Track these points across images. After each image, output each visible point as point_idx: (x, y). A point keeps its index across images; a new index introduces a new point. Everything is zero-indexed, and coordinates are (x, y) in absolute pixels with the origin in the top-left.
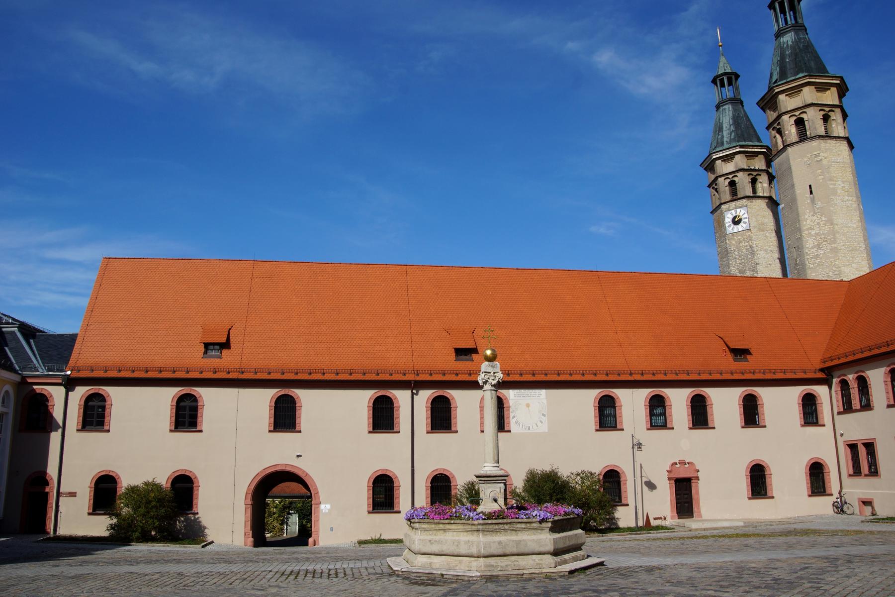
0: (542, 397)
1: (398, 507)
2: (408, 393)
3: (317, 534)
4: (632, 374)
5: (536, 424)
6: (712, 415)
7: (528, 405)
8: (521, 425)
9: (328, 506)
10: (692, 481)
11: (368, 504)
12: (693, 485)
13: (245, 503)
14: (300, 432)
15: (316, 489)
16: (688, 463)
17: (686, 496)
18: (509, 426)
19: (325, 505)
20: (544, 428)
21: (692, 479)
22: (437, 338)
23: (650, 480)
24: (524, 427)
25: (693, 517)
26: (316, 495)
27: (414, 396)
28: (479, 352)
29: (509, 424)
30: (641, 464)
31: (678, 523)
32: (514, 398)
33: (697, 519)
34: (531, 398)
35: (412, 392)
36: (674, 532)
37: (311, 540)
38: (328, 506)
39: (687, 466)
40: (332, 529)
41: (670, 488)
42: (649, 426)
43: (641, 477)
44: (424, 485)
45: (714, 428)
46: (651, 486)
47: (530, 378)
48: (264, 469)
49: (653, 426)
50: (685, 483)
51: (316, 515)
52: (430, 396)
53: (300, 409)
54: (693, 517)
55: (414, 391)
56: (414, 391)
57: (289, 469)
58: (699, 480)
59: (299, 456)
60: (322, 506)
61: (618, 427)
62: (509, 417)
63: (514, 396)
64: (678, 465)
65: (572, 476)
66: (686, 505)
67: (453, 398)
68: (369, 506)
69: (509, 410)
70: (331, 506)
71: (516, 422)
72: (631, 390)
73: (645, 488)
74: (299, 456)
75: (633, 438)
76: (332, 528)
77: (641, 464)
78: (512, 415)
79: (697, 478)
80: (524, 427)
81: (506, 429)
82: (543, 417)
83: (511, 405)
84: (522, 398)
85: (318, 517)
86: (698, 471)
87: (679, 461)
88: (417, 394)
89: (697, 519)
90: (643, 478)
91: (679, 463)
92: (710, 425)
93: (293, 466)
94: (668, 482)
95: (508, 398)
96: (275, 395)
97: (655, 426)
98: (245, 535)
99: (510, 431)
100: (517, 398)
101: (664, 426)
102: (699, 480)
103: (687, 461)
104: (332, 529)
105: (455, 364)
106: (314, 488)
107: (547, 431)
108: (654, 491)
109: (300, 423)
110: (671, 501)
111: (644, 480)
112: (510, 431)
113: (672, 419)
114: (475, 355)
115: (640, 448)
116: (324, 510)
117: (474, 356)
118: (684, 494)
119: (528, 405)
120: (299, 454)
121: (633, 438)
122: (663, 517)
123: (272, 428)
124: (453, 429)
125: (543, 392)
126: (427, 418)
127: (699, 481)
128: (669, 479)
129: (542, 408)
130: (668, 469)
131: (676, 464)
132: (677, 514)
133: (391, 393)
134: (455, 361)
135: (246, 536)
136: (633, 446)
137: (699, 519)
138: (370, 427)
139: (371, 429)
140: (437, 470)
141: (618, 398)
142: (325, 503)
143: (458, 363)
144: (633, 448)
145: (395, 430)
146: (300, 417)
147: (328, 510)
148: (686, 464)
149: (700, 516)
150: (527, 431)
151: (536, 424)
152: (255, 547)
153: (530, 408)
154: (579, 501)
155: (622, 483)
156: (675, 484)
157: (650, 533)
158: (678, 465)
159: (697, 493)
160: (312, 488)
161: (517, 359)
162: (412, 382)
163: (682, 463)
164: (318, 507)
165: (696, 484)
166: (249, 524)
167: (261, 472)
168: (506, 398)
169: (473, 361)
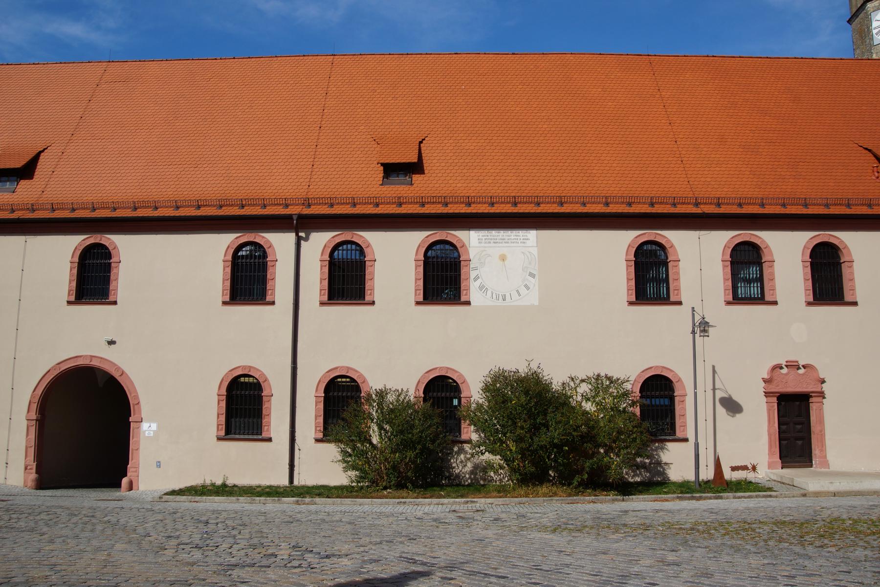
0: (529, 243)
1: (269, 430)
2: (291, 237)
3: (136, 471)
4: (700, 203)
5: (518, 291)
6: (852, 280)
7: (503, 258)
8: (489, 293)
9: (154, 426)
10: (811, 400)
11: (218, 425)
12: (813, 408)
13: (26, 417)
14: (115, 303)
15: (137, 397)
16: (804, 367)
17: (799, 427)
18: (468, 294)
19: (149, 425)
20: (532, 298)
21: (811, 397)
22: (359, 152)
23: (730, 395)
24: (494, 296)
25: (811, 466)
26: (136, 406)
27: (302, 242)
28: (426, 172)
29: (468, 289)
30: (714, 367)
31: (781, 477)
32: (478, 245)
33: (819, 470)
34: (509, 245)
35: (297, 235)
36: (770, 496)
37: (125, 481)
38: (154, 426)
39: (802, 371)
40: (159, 464)
41: (769, 411)
42: (730, 298)
43: (714, 389)
44: (313, 393)
45: (855, 304)
46: (732, 406)
47: (508, 209)
48: (58, 364)
49: (737, 299)
50: (798, 403)
51: (134, 439)
52: (329, 241)
53: (117, 267)
54: (811, 466)
55: (302, 234)
56: (302, 234)
57: (95, 363)
58: (824, 398)
59: (111, 343)
60: (145, 426)
61: (672, 299)
62: (468, 279)
63: (477, 241)
64: (785, 371)
65: (572, 384)
66: (800, 442)
67: (369, 246)
68: (220, 427)
69: (468, 266)
70: (158, 427)
71: (481, 287)
72: (698, 232)
73: (721, 410)
74: (111, 343)
75: (693, 315)
76: (159, 462)
77: (714, 367)
78: (473, 275)
79: (822, 395)
80: (494, 296)
81: (463, 298)
82: (531, 279)
83: (471, 257)
84: (492, 245)
85: (138, 442)
86: (823, 382)
87: (787, 362)
88: (306, 239)
89: (819, 470)
90: (717, 392)
91: (786, 366)
92: (848, 298)
93: (101, 358)
94: (764, 399)
95: (467, 244)
96: (80, 244)
97: (742, 299)
98: (26, 468)
99: (468, 303)
100: (483, 245)
101: (760, 300)
102: (824, 398)
103: (801, 363)
104: (159, 464)
105: (379, 189)
106: (132, 395)
107: (536, 303)
108: (738, 415)
109: (116, 290)
110: (770, 435)
111: (719, 394)
112: (468, 303)
113: (774, 286)
114: (417, 176)
115: (705, 331)
116: (147, 432)
117: (416, 178)
118: (796, 424)
119: (503, 258)
120: (110, 339)
121: (693, 315)
122: (750, 466)
123: (73, 298)
124: (368, 298)
125: (532, 235)
126: (321, 280)
127: (824, 400)
128: (767, 394)
129: (530, 263)
130: (766, 376)
131: (781, 368)
132: (780, 459)
133: (263, 237)
134: (382, 185)
135: (27, 471)
136: (693, 328)
137: (823, 470)
138: (226, 295)
139: (227, 298)
140: (336, 368)
141: (672, 246)
142: (151, 421)
143: (385, 188)
144: (693, 332)
145: (267, 300)
146: (117, 279)
147: (154, 431)
148: (799, 368)
149: (826, 464)
150: (500, 302)
151: (518, 291)
152: (37, 489)
153: (506, 262)
154: (575, 430)
155: (677, 399)
156: (779, 404)
157: (721, 498)
158: (785, 371)
159: (821, 421)
160: (130, 394)
161: (490, 181)
162: (295, 217)
163: (793, 366)
164: (139, 428)
165: (819, 404)
166: (32, 451)
167: (54, 368)
168: (463, 246)
169: (412, 184)
